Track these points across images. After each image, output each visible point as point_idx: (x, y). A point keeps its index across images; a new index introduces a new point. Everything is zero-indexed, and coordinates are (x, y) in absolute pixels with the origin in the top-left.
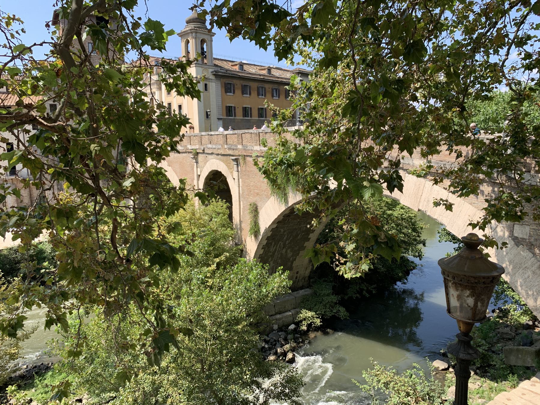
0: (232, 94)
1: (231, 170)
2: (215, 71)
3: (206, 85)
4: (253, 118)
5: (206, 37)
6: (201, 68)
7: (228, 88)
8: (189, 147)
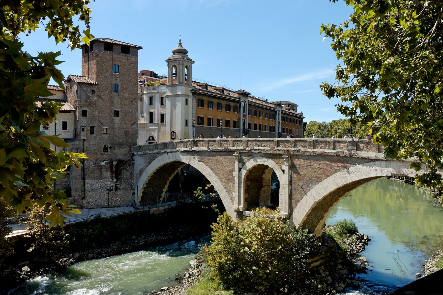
0: (202, 108)
3: (187, 100)
6: (184, 87)
7: (200, 103)
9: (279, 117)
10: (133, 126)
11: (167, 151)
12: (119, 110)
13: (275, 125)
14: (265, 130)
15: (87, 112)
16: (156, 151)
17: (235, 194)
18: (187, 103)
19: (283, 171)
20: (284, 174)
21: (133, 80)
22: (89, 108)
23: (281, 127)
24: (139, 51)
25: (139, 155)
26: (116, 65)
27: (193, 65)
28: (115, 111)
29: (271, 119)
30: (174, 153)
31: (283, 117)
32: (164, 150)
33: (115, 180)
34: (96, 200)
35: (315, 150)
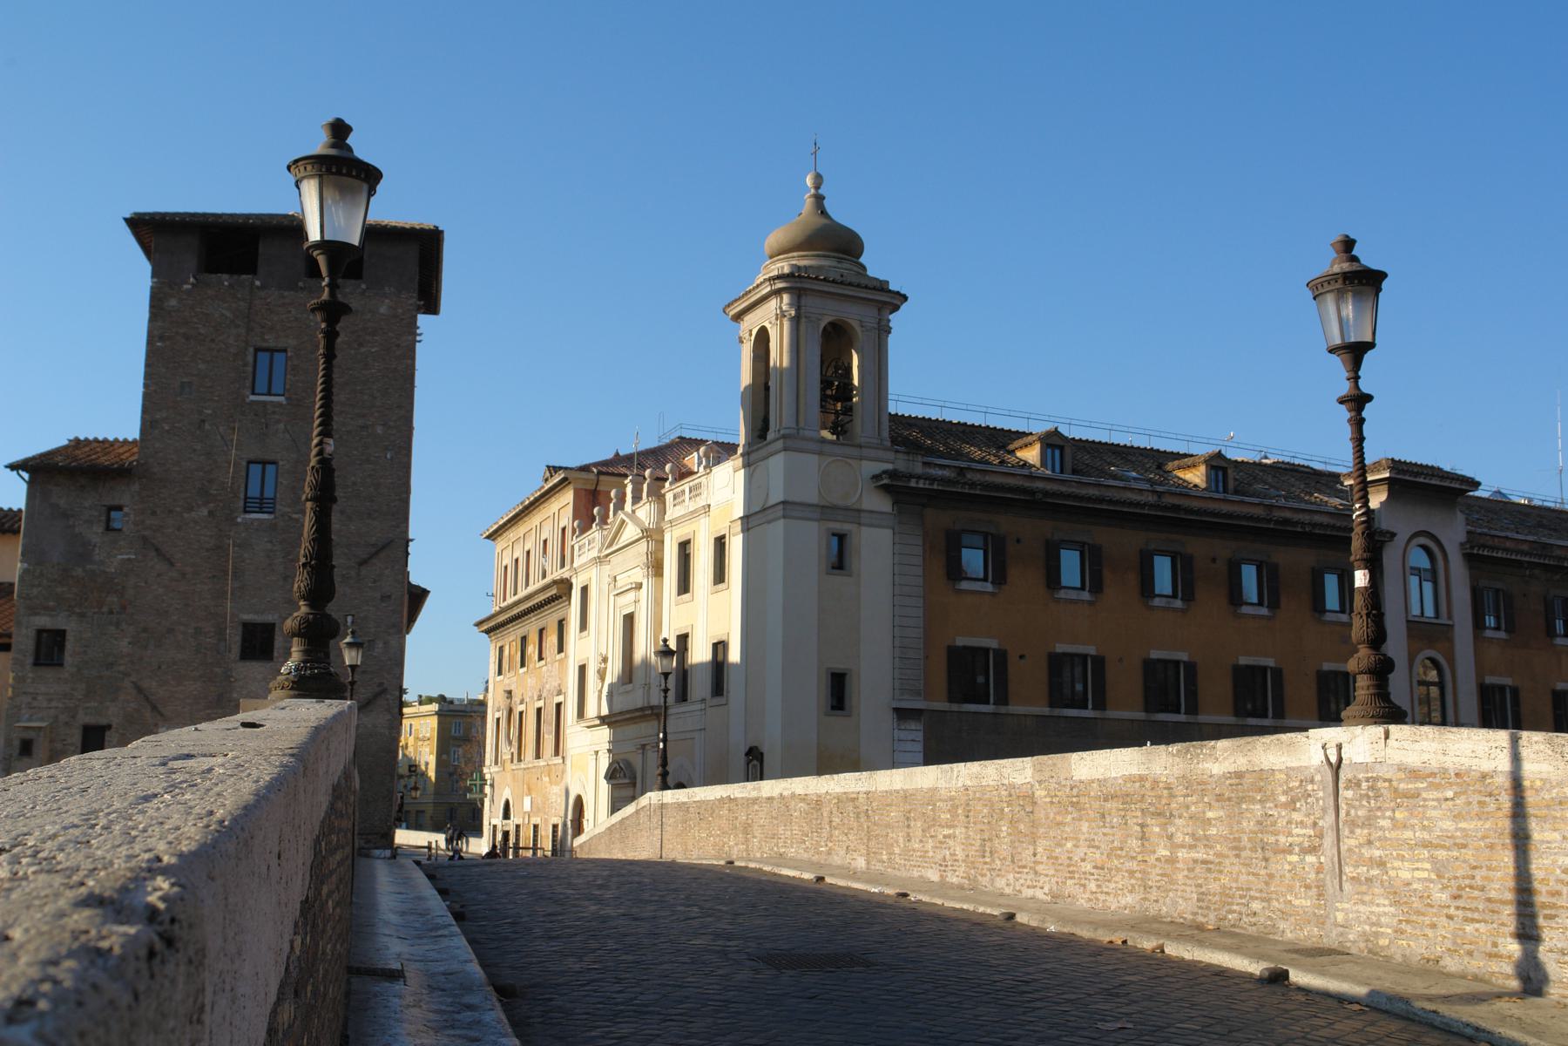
2: (893, 474)
3: (841, 538)
4: (1111, 714)
5: (854, 315)
6: (814, 458)
15: (70, 638)
18: (839, 563)
21: (379, 430)
22: (82, 615)
26: (272, 351)
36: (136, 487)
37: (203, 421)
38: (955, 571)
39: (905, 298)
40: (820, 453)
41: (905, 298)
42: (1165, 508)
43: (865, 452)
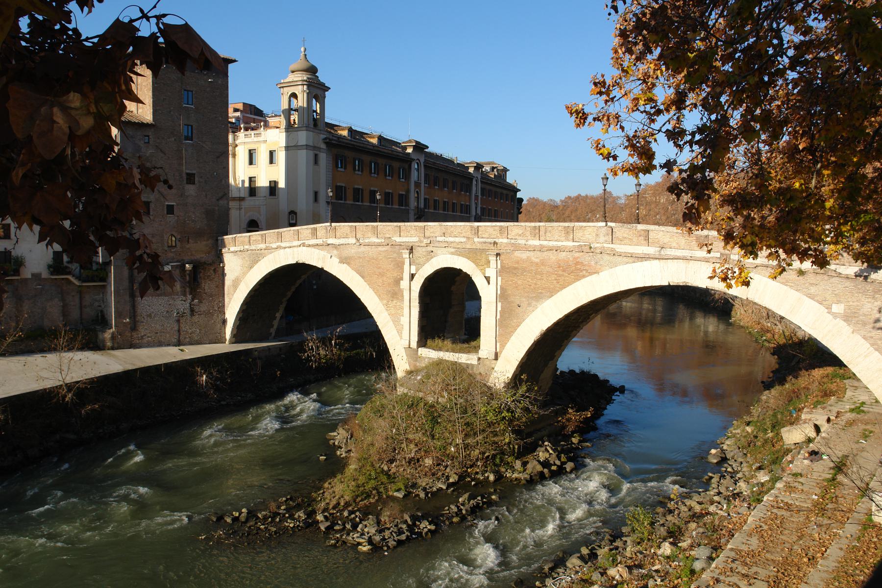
1: (482, 267)
5: (319, 92)
6: (311, 133)
8: (398, 239)
9: (476, 188)
10: (221, 202)
11: (283, 245)
12: (194, 172)
13: (470, 203)
14: (453, 211)
16: (263, 246)
17: (405, 320)
18: (316, 162)
19: (488, 279)
20: (489, 283)
21: (220, 118)
23: (479, 206)
24: (231, 66)
25: (232, 252)
26: (188, 91)
27: (326, 93)
28: (188, 174)
29: (463, 193)
30: (295, 249)
31: (482, 189)
32: (278, 244)
33: (189, 297)
34: (157, 333)
35: (542, 242)
36: (153, 130)
37: (170, 111)
38: (337, 166)
39: (330, 88)
40: (313, 132)
41: (330, 88)
42: (375, 150)
43: (322, 132)
